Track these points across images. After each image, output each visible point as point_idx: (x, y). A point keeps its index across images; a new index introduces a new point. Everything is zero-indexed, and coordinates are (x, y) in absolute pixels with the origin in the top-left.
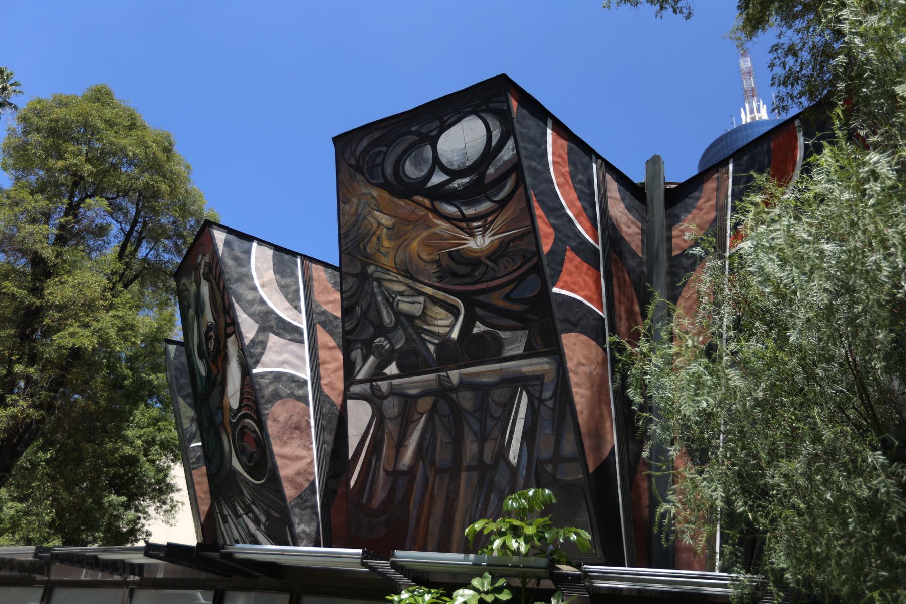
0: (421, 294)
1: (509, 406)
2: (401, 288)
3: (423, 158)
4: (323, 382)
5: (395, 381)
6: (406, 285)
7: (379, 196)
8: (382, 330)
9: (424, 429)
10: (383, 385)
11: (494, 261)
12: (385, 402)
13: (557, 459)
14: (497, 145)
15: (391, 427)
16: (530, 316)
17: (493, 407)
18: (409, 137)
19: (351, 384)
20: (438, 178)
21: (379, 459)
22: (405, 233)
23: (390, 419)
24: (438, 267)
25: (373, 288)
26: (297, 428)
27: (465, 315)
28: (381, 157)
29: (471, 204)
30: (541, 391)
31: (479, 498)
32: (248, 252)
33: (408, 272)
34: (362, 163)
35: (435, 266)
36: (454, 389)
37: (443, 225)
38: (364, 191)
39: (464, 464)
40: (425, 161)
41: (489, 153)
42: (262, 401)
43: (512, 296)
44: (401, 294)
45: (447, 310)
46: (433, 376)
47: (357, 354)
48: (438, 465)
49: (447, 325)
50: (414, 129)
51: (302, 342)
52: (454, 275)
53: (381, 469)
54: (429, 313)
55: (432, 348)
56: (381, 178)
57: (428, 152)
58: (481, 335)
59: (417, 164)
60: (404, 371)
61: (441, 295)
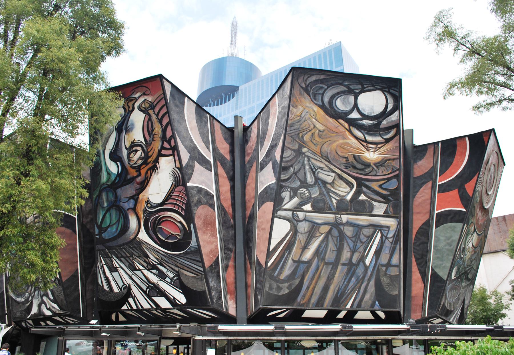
1: (370, 238)
2: (322, 165)
3: (348, 101)
4: (222, 197)
5: (308, 214)
6: (325, 164)
7: (318, 111)
8: (304, 184)
9: (322, 242)
10: (301, 215)
11: (377, 167)
12: (300, 224)
13: (389, 265)
14: (390, 111)
15: (301, 238)
16: (390, 198)
17: (362, 237)
18: (342, 87)
19: (279, 210)
20: (355, 115)
21: (290, 253)
22: (331, 137)
23: (301, 233)
24: (346, 161)
25: (304, 160)
26: (209, 224)
27: (356, 189)
28: (323, 90)
29: (370, 135)
30: (387, 234)
31: (345, 279)
32: (183, 104)
33: (328, 158)
34: (309, 89)
35: (345, 160)
36: (342, 224)
37: (354, 140)
38: (308, 105)
39: (341, 262)
40: (349, 103)
41: (384, 114)
42: (193, 205)
43: (383, 186)
44: (322, 169)
45: (347, 184)
46: (333, 216)
47: (286, 195)
48: (326, 261)
49: (345, 192)
50: (346, 83)
51: (211, 171)
52: (354, 167)
53: (290, 259)
54: (336, 183)
55: (334, 201)
56: (320, 102)
57: (352, 98)
58: (363, 201)
59: (344, 102)
60: (316, 209)
61: (345, 176)
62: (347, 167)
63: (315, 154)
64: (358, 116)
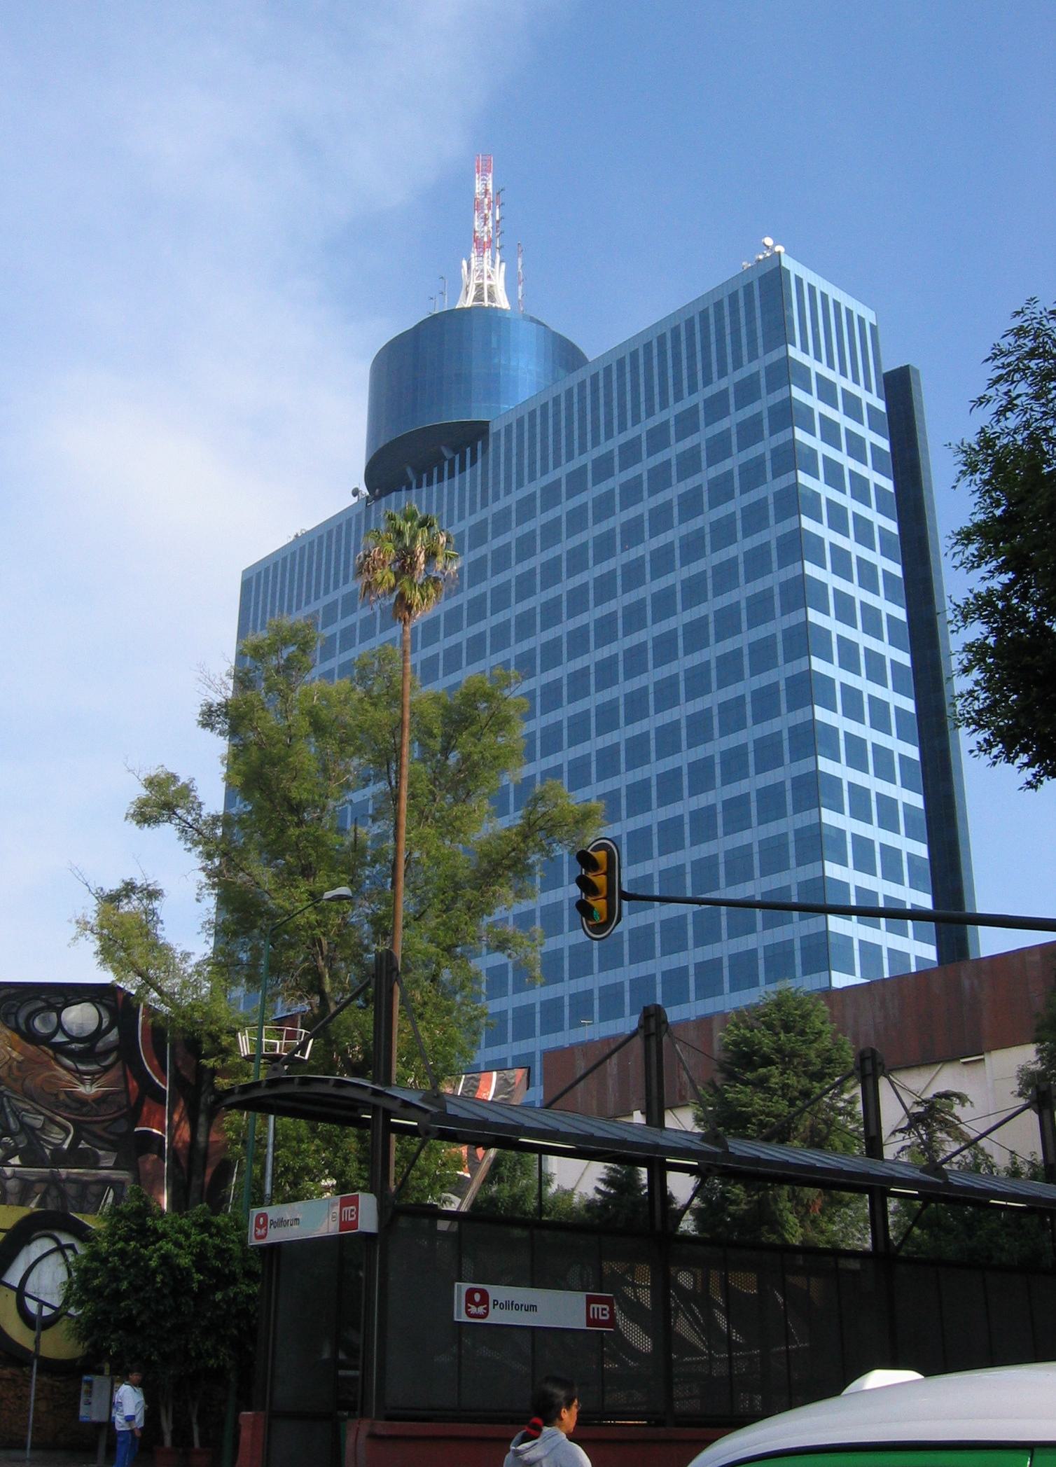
0: (41, 1114)
1: (100, 1196)
20: (60, 1038)
29: (83, 1063)
41: (99, 1033)
44: (27, 1111)
57: (54, 1015)
59: (45, 1022)
62: (58, 1107)
63: (15, 1092)
64: (66, 1039)
